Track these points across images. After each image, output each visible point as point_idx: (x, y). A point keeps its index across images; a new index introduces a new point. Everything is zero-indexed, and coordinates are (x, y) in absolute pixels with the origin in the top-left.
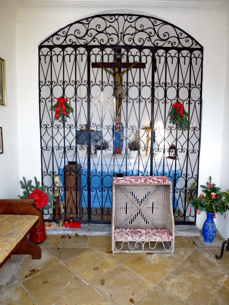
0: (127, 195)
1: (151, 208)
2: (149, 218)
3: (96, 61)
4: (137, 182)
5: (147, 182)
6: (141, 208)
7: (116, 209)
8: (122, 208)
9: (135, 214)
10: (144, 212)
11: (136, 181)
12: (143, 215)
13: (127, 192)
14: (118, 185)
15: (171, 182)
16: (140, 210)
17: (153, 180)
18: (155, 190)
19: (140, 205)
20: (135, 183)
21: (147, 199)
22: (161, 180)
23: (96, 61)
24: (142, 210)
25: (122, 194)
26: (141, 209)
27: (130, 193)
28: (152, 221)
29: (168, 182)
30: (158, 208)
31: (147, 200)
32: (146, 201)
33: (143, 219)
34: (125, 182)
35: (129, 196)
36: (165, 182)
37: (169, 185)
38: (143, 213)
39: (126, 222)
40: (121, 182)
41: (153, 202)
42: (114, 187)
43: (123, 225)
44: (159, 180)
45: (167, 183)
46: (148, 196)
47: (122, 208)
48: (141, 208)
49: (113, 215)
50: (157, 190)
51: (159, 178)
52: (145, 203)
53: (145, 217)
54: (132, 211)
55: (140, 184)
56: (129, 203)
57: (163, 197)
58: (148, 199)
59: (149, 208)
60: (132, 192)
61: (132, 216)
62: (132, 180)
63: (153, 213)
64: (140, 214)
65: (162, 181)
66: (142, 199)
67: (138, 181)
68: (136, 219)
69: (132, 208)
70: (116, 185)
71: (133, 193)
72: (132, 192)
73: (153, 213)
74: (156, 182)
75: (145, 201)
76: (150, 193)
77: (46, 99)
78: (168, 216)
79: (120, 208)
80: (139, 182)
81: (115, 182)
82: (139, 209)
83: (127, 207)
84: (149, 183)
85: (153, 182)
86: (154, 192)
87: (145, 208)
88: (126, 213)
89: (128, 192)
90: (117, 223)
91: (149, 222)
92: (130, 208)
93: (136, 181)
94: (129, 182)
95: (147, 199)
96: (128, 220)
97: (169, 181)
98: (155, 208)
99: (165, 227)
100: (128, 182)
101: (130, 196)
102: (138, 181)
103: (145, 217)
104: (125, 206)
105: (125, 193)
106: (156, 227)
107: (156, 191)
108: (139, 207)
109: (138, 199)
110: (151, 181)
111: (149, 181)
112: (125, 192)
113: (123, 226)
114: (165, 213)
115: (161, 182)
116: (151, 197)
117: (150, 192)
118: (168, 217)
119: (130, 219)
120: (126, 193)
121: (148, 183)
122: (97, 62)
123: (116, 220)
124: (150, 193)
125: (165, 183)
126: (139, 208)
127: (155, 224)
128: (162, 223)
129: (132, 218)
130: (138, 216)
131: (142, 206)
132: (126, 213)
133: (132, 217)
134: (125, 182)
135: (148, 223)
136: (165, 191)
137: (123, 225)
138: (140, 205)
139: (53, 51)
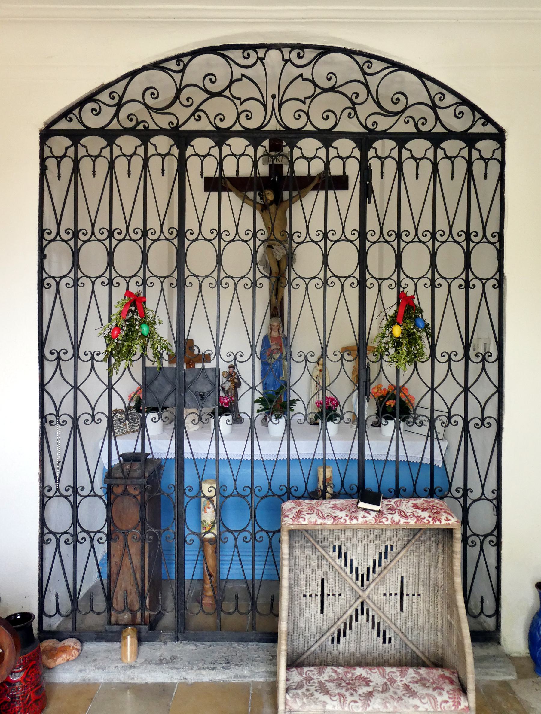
0: (323, 557)
1: (396, 594)
2: (393, 627)
3: (237, 171)
4: (355, 521)
5: (384, 520)
6: (368, 597)
7: (292, 598)
8: (311, 596)
9: (347, 615)
10: (375, 608)
11: (351, 518)
12: (373, 617)
13: (323, 548)
14: (299, 530)
15: (456, 519)
16: (362, 603)
17: (402, 514)
18: (409, 541)
19: (362, 585)
20: (348, 522)
21: (385, 568)
22: (425, 514)
23: (237, 171)
24: (370, 603)
25: (310, 553)
26: (367, 600)
27: (334, 551)
28: (400, 634)
29: (448, 520)
30: (419, 595)
31: (385, 572)
32: (382, 575)
33: (373, 628)
34: (319, 521)
35: (330, 560)
36: (439, 520)
37: (452, 529)
38: (373, 610)
39: (323, 639)
40: (306, 522)
41: (402, 578)
42: (285, 538)
43: (313, 649)
44: (420, 513)
45: (443, 522)
46: (386, 558)
47: (311, 596)
48: (368, 597)
49: (284, 613)
50: (413, 541)
51: (419, 508)
52: (378, 580)
53: (379, 623)
54: (339, 607)
55: (364, 527)
56: (331, 580)
57: (433, 561)
58: (388, 568)
59: (391, 594)
60: (340, 548)
61: (339, 619)
62: (338, 513)
63: (402, 609)
64: (362, 613)
65: (430, 517)
66: (368, 569)
67: (356, 518)
68: (351, 628)
69: (340, 595)
70: (292, 533)
71: (343, 548)
72: (340, 548)
73: (402, 609)
74: (412, 521)
75: (379, 574)
76: (392, 550)
77: (484, 281)
78: (450, 624)
79: (305, 596)
80: (361, 520)
81: (288, 522)
82: (360, 600)
83: (326, 593)
84: (389, 522)
85: (403, 521)
86: (405, 546)
87: (381, 595)
88: (322, 612)
89: (328, 547)
90: (295, 643)
91: (390, 639)
92: (334, 595)
93: (351, 518)
94: (329, 521)
95: (385, 568)
96: (328, 634)
97: (450, 517)
98: (408, 595)
99: (442, 654)
100: (326, 521)
101: (332, 558)
102: (356, 518)
103: (379, 623)
104: (320, 589)
105: (319, 551)
106: (415, 653)
107: (410, 544)
108: (361, 593)
109: (357, 569)
110: (396, 517)
111: (390, 516)
112: (318, 547)
113: (313, 652)
114: (440, 610)
115: (425, 521)
116: (395, 561)
117: (392, 546)
118: (452, 627)
119: (334, 630)
120: (321, 549)
121: (386, 523)
122: (241, 174)
123: (290, 633)
124: (392, 550)
125: (438, 523)
126: (360, 596)
127: (411, 645)
128: (431, 642)
129: (340, 625)
130: (357, 620)
131: (369, 589)
132: (322, 612)
133: (339, 623)
134: (319, 521)
135: (390, 641)
136: (437, 544)
137: (313, 649)
138: (362, 585)
139: (151, 143)
